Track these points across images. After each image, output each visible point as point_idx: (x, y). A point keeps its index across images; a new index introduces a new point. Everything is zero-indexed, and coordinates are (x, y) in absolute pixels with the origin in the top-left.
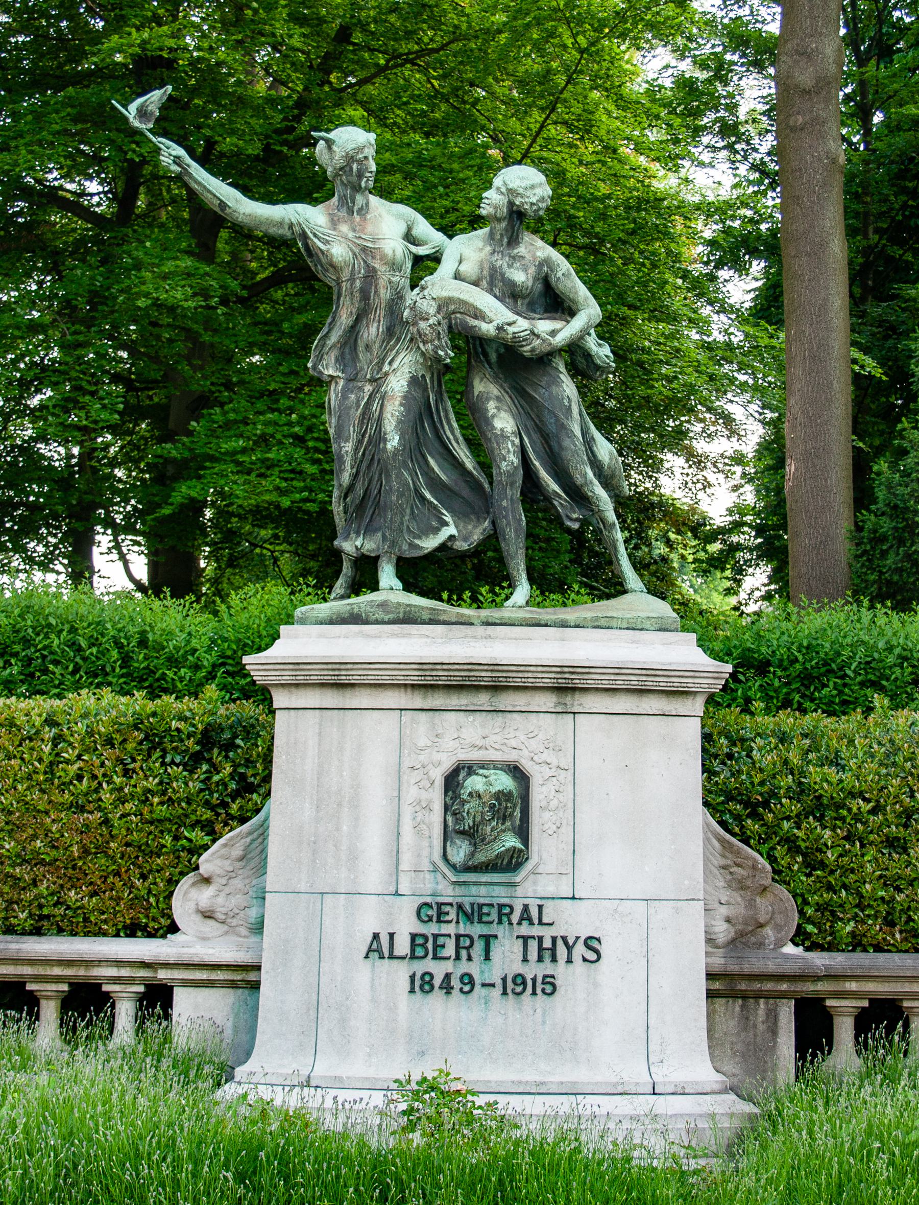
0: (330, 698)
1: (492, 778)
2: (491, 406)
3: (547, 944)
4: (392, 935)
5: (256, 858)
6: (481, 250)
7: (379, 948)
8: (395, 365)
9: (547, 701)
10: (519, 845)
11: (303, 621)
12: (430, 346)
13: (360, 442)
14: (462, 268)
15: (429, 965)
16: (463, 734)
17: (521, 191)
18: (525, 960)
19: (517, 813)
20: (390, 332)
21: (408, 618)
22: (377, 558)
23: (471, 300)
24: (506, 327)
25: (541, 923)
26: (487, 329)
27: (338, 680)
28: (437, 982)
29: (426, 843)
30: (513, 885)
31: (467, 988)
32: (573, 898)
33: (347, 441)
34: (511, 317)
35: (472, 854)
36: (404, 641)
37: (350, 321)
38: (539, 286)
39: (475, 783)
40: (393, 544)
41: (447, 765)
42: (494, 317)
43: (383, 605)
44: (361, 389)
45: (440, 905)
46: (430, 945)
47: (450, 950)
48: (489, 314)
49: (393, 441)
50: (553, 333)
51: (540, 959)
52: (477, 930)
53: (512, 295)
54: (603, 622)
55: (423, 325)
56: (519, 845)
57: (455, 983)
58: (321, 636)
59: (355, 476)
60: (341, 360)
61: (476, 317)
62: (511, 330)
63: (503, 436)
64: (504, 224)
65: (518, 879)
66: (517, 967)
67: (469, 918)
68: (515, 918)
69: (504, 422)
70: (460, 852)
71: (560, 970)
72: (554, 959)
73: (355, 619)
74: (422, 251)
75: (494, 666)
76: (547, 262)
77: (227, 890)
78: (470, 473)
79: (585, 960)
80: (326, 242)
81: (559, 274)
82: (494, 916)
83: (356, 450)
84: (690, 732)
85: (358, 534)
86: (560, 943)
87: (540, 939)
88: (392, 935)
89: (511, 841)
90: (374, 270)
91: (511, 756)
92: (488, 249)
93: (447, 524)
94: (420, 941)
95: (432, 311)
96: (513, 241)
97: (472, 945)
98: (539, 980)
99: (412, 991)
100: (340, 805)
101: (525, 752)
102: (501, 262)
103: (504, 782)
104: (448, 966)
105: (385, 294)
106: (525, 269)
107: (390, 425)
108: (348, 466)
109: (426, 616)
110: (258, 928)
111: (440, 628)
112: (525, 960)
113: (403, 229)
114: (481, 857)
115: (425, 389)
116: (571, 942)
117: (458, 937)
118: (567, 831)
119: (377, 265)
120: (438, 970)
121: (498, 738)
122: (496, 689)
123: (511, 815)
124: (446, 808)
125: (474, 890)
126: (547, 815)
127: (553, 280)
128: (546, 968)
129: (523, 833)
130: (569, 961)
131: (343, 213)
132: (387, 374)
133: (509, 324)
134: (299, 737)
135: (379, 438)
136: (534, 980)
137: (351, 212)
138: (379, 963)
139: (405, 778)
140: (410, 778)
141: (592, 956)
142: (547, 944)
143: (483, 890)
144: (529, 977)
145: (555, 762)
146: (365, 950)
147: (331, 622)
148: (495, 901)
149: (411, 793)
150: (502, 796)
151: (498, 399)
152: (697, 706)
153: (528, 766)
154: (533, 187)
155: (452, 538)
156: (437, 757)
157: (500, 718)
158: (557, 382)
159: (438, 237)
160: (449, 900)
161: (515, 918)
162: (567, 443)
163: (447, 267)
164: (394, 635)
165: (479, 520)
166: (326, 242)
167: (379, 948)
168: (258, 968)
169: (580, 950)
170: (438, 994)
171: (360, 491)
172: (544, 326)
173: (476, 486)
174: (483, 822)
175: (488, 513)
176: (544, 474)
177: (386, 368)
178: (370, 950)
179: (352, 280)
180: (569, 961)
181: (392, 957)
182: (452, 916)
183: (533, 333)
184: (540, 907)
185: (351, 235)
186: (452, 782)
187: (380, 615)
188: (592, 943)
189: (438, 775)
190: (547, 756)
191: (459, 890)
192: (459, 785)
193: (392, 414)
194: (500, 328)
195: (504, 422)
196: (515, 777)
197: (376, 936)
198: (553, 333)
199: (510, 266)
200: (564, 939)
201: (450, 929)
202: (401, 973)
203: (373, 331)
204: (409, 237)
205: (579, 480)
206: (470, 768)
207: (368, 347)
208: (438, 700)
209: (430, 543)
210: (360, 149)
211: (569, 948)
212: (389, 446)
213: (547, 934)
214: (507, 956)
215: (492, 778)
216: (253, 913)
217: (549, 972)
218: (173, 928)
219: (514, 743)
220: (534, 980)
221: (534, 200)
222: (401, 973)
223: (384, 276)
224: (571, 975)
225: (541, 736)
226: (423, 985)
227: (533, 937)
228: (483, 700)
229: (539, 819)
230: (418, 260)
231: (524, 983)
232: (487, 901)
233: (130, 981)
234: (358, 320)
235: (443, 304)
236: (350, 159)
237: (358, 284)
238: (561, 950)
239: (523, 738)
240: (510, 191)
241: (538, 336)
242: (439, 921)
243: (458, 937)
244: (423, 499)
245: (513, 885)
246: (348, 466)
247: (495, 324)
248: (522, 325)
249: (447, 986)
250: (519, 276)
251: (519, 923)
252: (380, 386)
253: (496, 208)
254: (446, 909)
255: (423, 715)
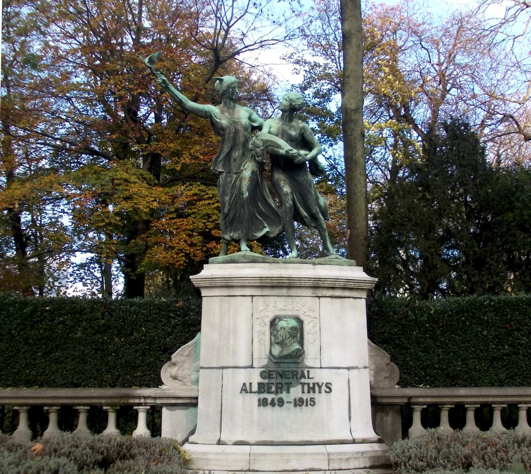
0: (225, 292)
1: (289, 322)
2: (282, 183)
3: (311, 386)
4: (251, 384)
5: (195, 355)
7: (245, 389)
8: (246, 167)
9: (309, 292)
10: (300, 348)
11: (213, 263)
12: (260, 158)
13: (232, 196)
14: (272, 130)
15: (265, 395)
16: (277, 305)
18: (303, 392)
19: (299, 335)
20: (244, 155)
21: (254, 261)
22: (239, 240)
25: (309, 378)
26: (282, 152)
27: (227, 284)
28: (269, 401)
29: (263, 347)
30: (298, 363)
31: (281, 404)
32: (321, 368)
33: (227, 196)
34: (291, 148)
35: (282, 351)
36: (253, 269)
37: (228, 150)
38: (300, 138)
39: (282, 324)
40: (246, 234)
41: (271, 317)
43: (244, 256)
44: (232, 176)
45: (270, 371)
46: (266, 388)
47: (273, 389)
49: (246, 195)
50: (306, 155)
51: (309, 392)
52: (285, 381)
53: (290, 140)
54: (328, 262)
55: (258, 150)
56: (300, 348)
57: (276, 402)
58: (220, 268)
59: (229, 210)
60: (224, 165)
61: (277, 148)
62: (291, 152)
63: (287, 194)
64: (287, 113)
65: (299, 361)
66: (300, 395)
67: (281, 376)
68: (299, 376)
69: (287, 189)
70: (277, 350)
71: (316, 396)
72: (314, 392)
73: (233, 261)
74: (255, 124)
75: (290, 278)
77: (182, 368)
78: (274, 209)
79: (326, 392)
80: (220, 119)
82: (291, 376)
83: (230, 199)
84: (362, 304)
85: (231, 232)
86: (316, 386)
87: (309, 384)
88: (251, 384)
89: (297, 346)
90: (238, 130)
91: (296, 313)
92: (281, 123)
93: (266, 227)
94: (262, 386)
95: (261, 144)
96: (291, 120)
97: (282, 387)
98: (309, 400)
99: (259, 406)
100: (229, 333)
101: (301, 312)
103: (293, 323)
104: (273, 396)
105: (242, 139)
106: (295, 130)
107: (244, 188)
108: (227, 205)
109: (261, 260)
110: (197, 381)
111: (267, 264)
112: (303, 392)
113: (247, 115)
114: (285, 352)
115: (257, 176)
116: (320, 384)
117: (277, 384)
118: (318, 342)
119: (239, 128)
120: (270, 397)
121: (290, 306)
122: (290, 287)
123: (296, 336)
124: (271, 334)
125: (282, 365)
126: (310, 336)
127: (305, 135)
128: (311, 395)
129: (301, 342)
130: (320, 392)
131: (226, 109)
132: (242, 170)
134: (212, 307)
135: (241, 193)
136: (307, 400)
137: (229, 108)
138: (246, 395)
139: (254, 322)
140: (256, 323)
141: (328, 390)
142: (311, 386)
143: (286, 365)
144: (305, 399)
145: (312, 316)
146: (240, 389)
147: (224, 263)
148: (290, 369)
149: (257, 328)
150: (293, 328)
151: (284, 181)
152: (364, 295)
153: (302, 317)
154: (299, 99)
155: (268, 232)
156: (267, 314)
157: (291, 299)
158: (307, 175)
159: (261, 120)
160: (272, 369)
161: (299, 376)
162: (310, 197)
163: (265, 130)
164: (249, 267)
165: (277, 226)
166: (220, 119)
167: (245, 389)
168: (197, 398)
169: (324, 388)
170: (269, 407)
171: (231, 215)
172: (302, 152)
173: (276, 214)
174: (286, 338)
175: (281, 223)
176: (301, 209)
177: (242, 168)
178: (242, 390)
179: (230, 133)
180: (320, 392)
181: (251, 392)
182: (274, 376)
184: (308, 372)
185: (229, 117)
186: (273, 323)
187: (243, 260)
188: (329, 386)
189: (268, 321)
190: (309, 313)
191: (276, 365)
192: (276, 325)
193: (245, 184)
194: (287, 152)
195: (287, 189)
196: (297, 321)
197: (244, 384)
198: (306, 155)
199: (290, 129)
200: (318, 384)
201: (274, 381)
202: (255, 398)
203: (236, 154)
204: (250, 118)
205: (314, 211)
206: (280, 318)
207: (235, 160)
208: (267, 292)
209: (260, 234)
210: (232, 83)
211: (320, 387)
212: (244, 196)
213: (311, 382)
214: (296, 392)
215: (289, 322)
216: (194, 377)
217: (312, 397)
218: (162, 384)
219: (296, 308)
220: (307, 400)
222: (255, 398)
223: (242, 132)
224: (321, 398)
225: (307, 306)
226: (263, 403)
227: (305, 383)
228: (284, 291)
229: (307, 337)
230: (254, 128)
231: (303, 402)
232: (288, 369)
233: (146, 404)
234: (231, 150)
235: (265, 142)
236: (229, 87)
237: (232, 135)
238: (317, 388)
239: (300, 306)
240: (291, 100)
241: (300, 155)
242: (269, 378)
243: (277, 384)
244: (257, 217)
245: (298, 363)
246: (227, 205)
248: (295, 151)
249: (273, 404)
250: (293, 133)
251: (301, 378)
252: (239, 175)
253: (285, 106)
254: (272, 373)
255: (261, 298)
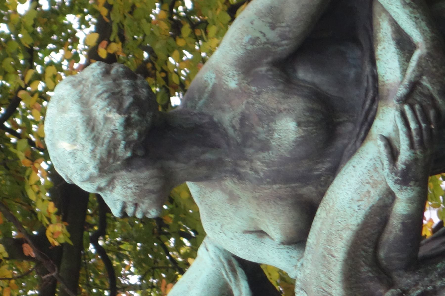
6: (233, 198)
17: (101, 150)
23: (347, 235)
24: (400, 165)
42: (381, 188)
48: (375, 196)
76: (246, 67)
81: (272, 35)
102: (260, 163)
106: (270, 116)
133: (393, 154)
154: (90, 124)
183: (406, 99)
198: (404, 44)
199: (265, 146)
221: (117, 119)
241: (414, 86)
247: (394, 188)
248: (388, 121)
